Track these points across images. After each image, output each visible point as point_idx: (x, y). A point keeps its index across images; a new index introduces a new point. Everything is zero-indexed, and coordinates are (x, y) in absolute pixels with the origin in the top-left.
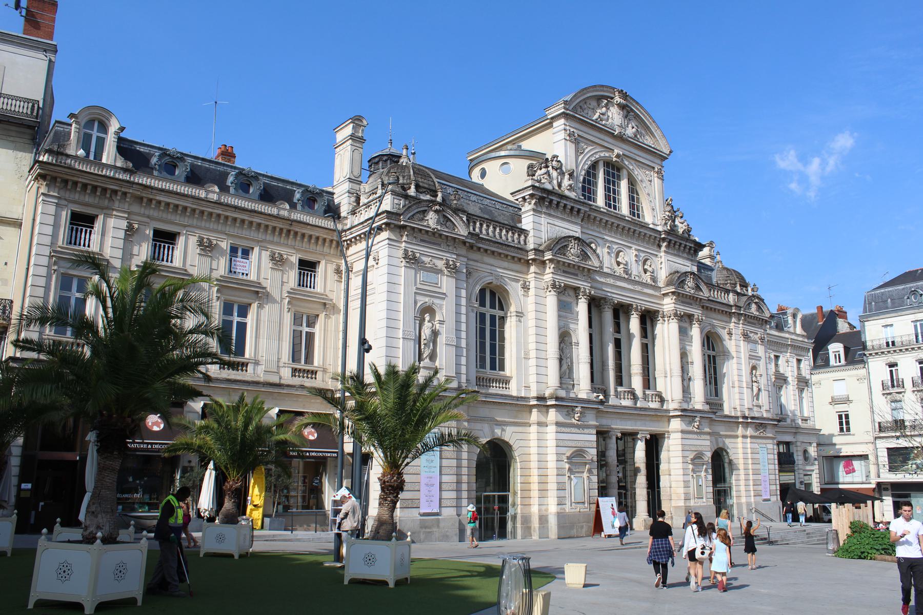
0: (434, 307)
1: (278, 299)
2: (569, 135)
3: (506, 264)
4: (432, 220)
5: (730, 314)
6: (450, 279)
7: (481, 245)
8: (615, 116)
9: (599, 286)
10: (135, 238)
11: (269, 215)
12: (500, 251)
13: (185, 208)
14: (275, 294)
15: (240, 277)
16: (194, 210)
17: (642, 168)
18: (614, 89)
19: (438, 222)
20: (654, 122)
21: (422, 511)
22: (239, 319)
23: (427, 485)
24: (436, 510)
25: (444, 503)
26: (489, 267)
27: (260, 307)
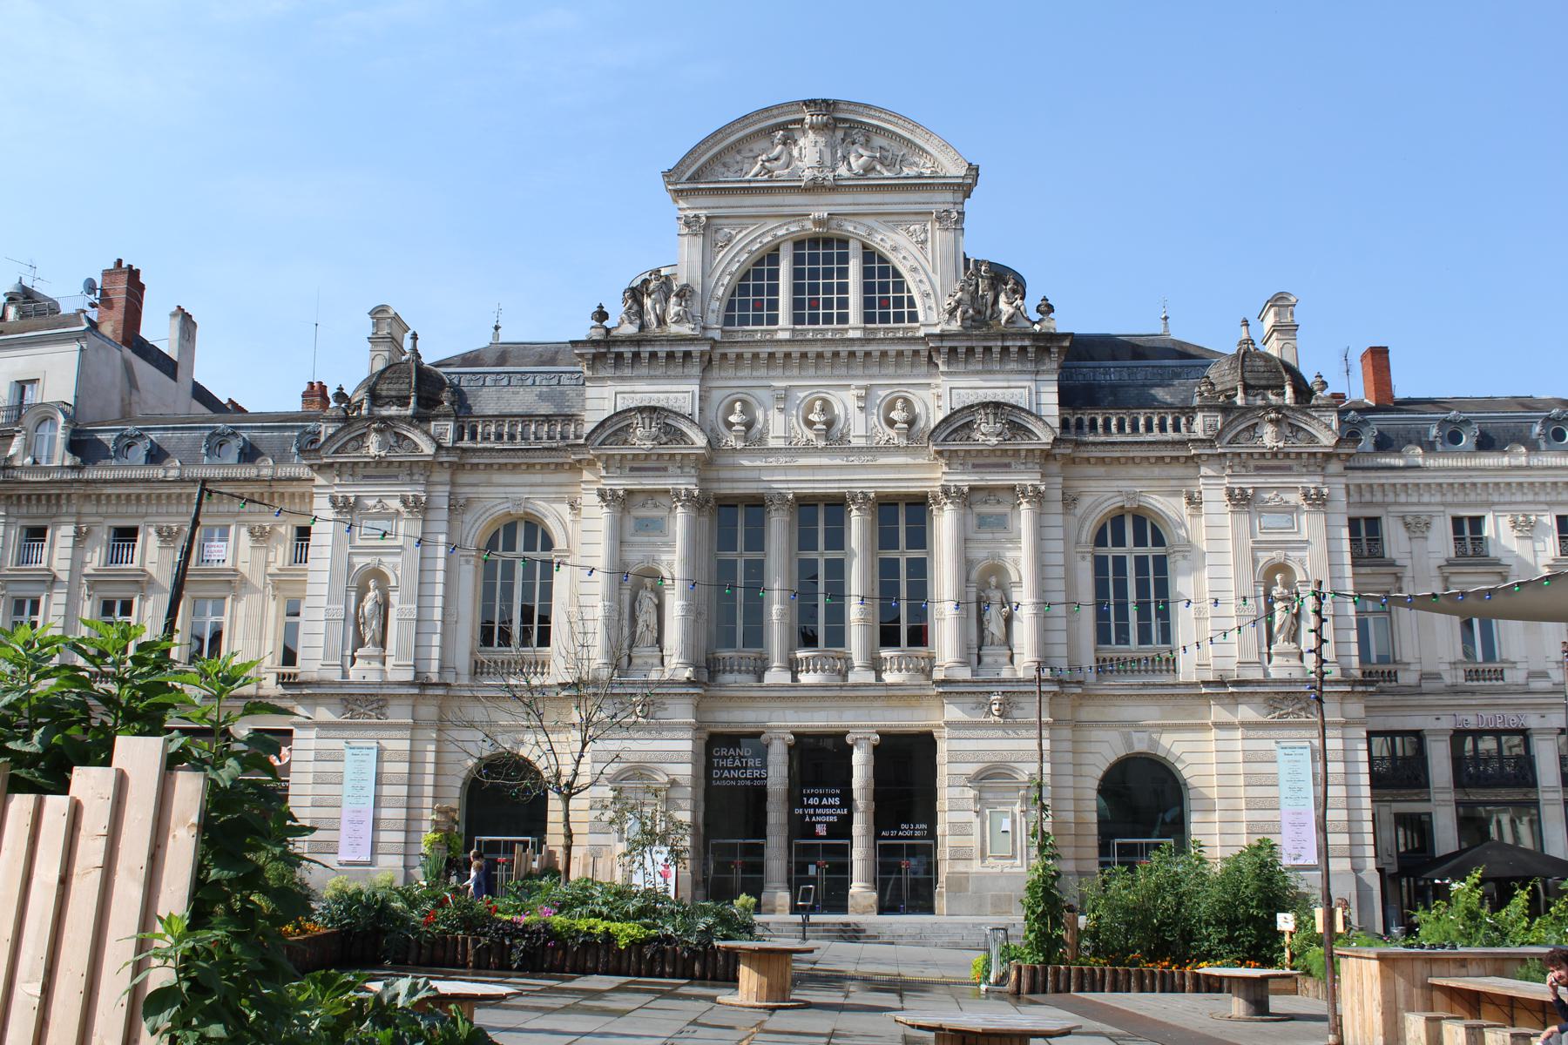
0: (383, 568)
1: (260, 585)
2: (687, 224)
3: (538, 478)
4: (373, 445)
5: (1194, 461)
6: (413, 523)
7: (476, 461)
8: (808, 151)
9: (754, 474)
10: (88, 543)
11: (246, 480)
12: (516, 461)
13: (138, 496)
14: (257, 580)
15: (215, 565)
16: (149, 496)
17: (898, 224)
18: (797, 103)
19: (381, 447)
20: (918, 126)
21: (343, 858)
22: (213, 619)
23: (352, 822)
24: (366, 858)
25: (381, 848)
26: (502, 489)
27: (236, 599)
